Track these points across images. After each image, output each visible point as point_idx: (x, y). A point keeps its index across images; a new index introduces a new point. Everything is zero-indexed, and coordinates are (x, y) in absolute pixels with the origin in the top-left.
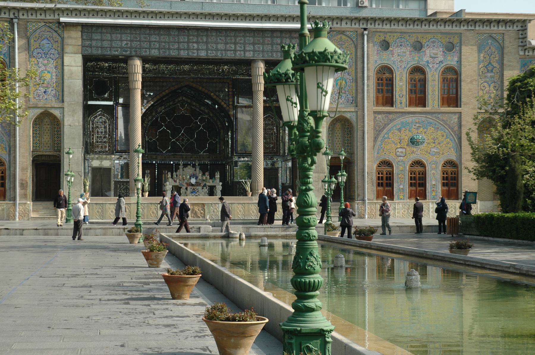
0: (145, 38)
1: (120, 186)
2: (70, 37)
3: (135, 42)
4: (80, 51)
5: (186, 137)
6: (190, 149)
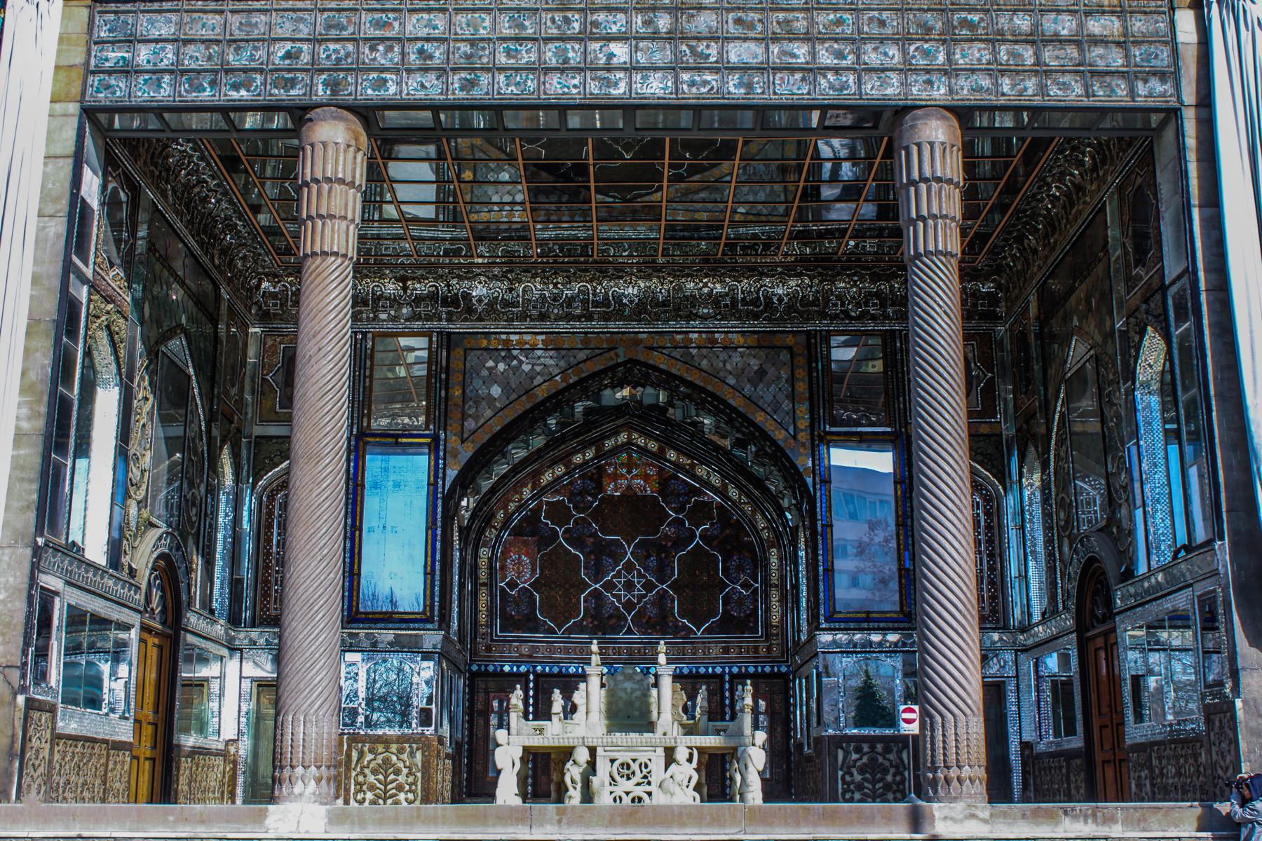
0: (378, 24)
1: (361, 755)
3: (332, 46)
4: (76, 89)
5: (640, 575)
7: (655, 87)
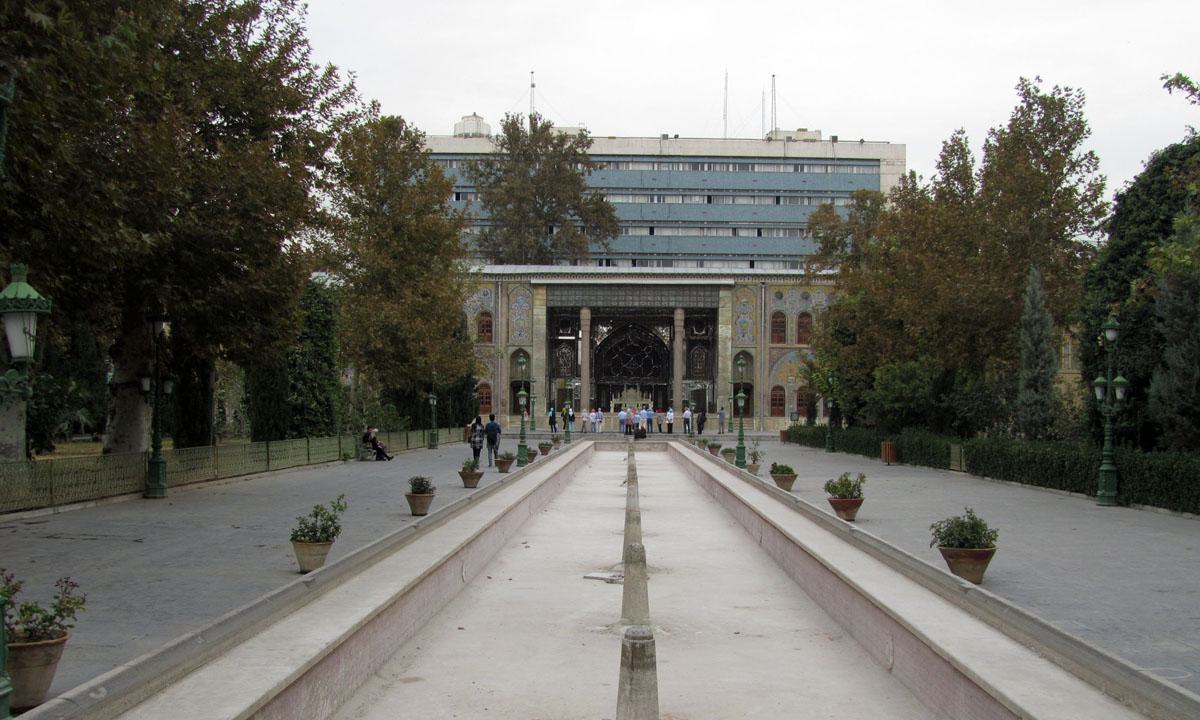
2: (538, 294)
6: (638, 373)
7: (636, 304)
